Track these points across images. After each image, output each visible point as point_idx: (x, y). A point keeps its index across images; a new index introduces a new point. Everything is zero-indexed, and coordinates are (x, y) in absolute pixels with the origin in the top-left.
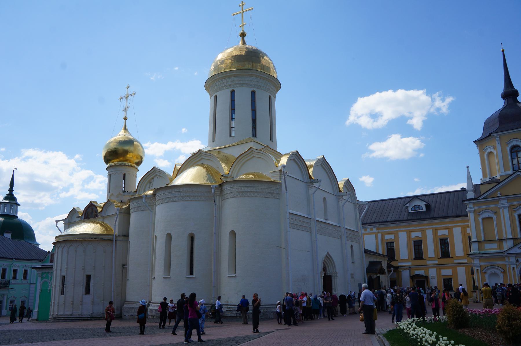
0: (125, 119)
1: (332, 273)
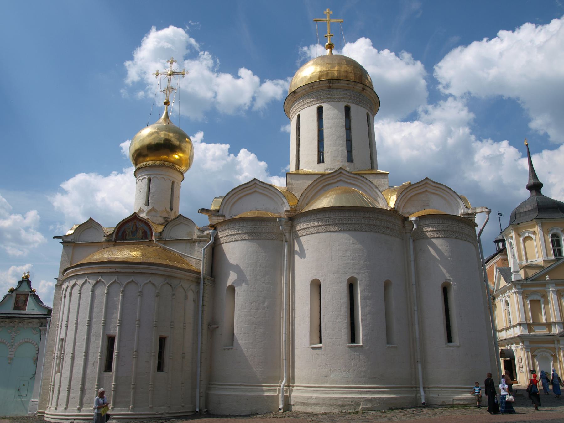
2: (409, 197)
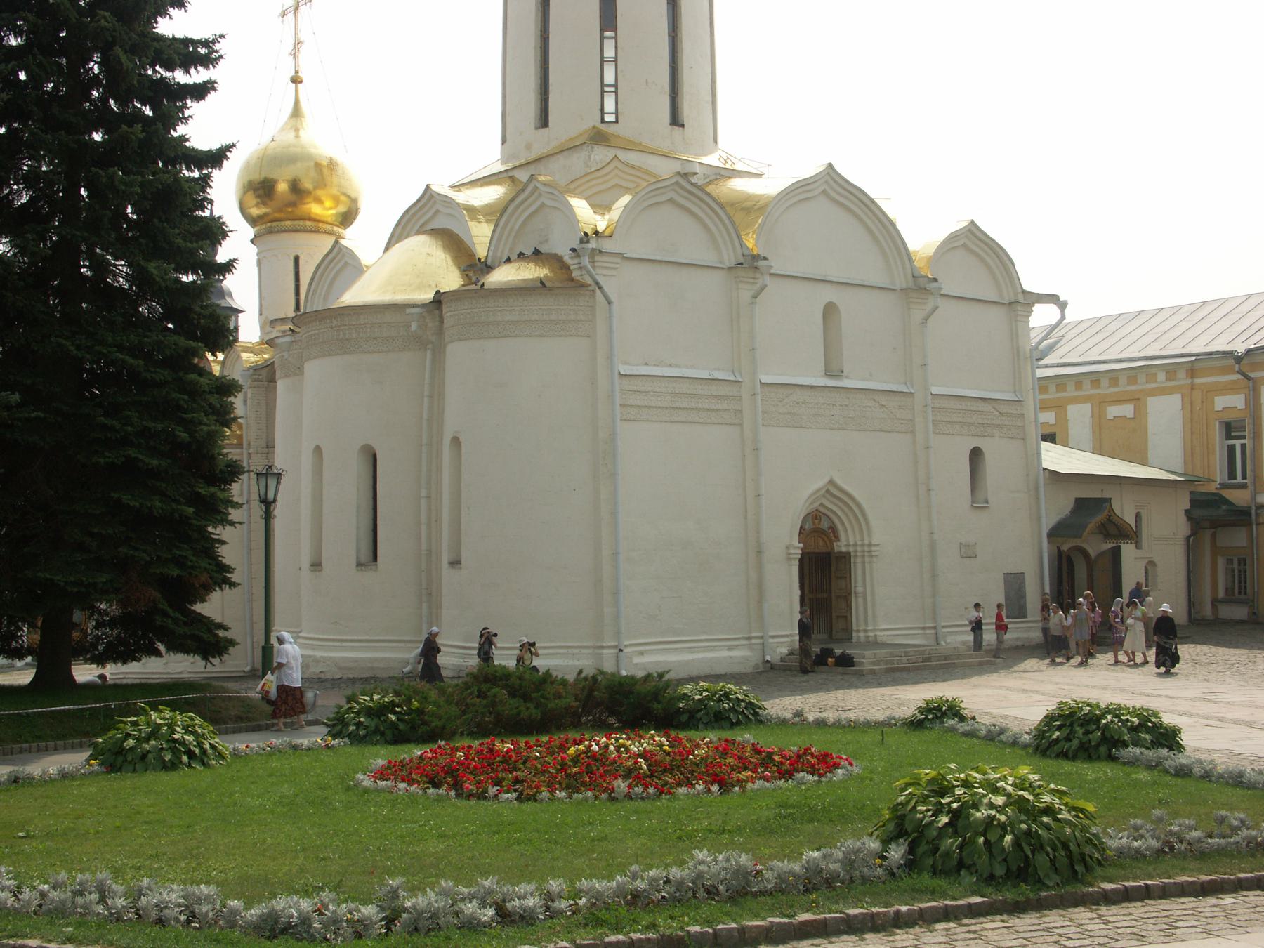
0: (296, 80)
1: (855, 545)
2: (517, 227)
